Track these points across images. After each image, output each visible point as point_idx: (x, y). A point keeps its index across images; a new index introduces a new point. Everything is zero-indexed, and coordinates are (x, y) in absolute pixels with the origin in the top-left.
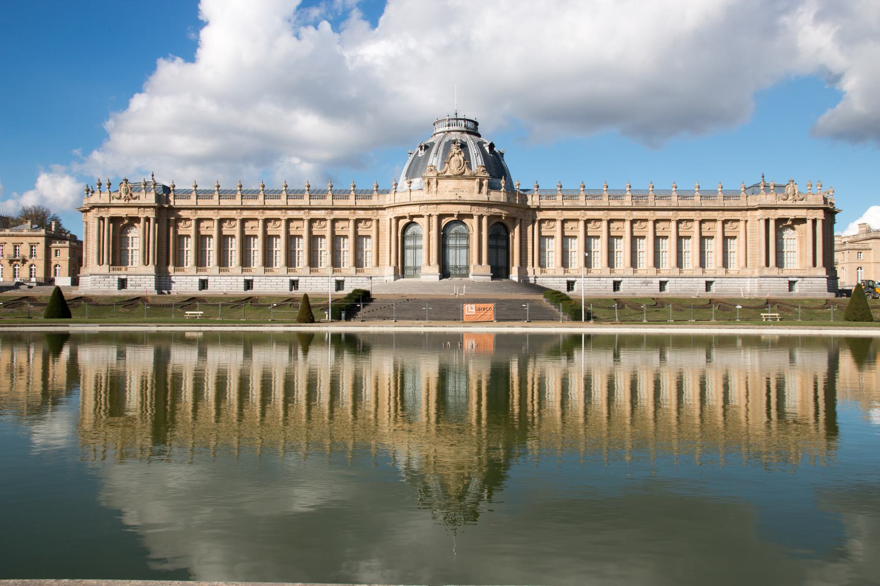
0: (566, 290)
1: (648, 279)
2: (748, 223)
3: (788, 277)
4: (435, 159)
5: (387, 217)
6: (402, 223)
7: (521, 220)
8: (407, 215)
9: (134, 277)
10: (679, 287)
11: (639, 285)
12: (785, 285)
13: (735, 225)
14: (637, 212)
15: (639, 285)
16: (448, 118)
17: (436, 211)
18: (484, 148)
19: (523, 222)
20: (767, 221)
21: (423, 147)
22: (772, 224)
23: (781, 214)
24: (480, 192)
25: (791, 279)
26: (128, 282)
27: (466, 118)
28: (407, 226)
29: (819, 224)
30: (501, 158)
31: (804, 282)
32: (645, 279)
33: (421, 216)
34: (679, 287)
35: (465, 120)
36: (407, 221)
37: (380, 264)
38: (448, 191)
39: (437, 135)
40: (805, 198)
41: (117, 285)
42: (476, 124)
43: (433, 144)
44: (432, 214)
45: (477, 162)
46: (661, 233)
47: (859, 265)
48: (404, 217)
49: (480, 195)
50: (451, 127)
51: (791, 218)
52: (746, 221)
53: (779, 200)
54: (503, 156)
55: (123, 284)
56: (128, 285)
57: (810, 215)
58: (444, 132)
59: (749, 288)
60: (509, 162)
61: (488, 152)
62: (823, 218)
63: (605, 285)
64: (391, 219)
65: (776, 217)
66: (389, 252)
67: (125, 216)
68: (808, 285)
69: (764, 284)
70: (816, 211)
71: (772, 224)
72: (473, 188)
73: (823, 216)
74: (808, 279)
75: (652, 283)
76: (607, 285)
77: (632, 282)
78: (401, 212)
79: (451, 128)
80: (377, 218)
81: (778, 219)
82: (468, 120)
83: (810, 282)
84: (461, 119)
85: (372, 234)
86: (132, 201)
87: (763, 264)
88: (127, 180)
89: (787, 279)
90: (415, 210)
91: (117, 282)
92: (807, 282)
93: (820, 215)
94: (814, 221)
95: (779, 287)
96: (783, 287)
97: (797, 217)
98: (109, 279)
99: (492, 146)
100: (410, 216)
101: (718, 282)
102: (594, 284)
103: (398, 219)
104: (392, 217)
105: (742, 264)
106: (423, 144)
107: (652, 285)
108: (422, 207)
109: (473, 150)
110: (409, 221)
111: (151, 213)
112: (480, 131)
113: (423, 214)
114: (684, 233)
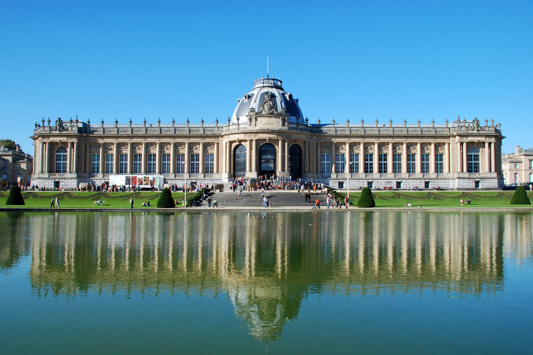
0: (338, 187)
1: (389, 180)
2: (451, 145)
3: (475, 179)
4: (255, 104)
5: (224, 141)
6: (234, 145)
7: (309, 143)
8: (237, 140)
9: (64, 180)
11: (384, 184)
15: (384, 184)
16: (263, 78)
17: (254, 137)
18: (286, 97)
19: (310, 144)
20: (462, 144)
21: (247, 97)
22: (464, 145)
23: (470, 139)
24: (283, 125)
25: (476, 180)
26: (60, 183)
27: (275, 78)
28: (237, 147)
29: (492, 146)
30: (296, 103)
31: (484, 181)
32: (387, 180)
33: (246, 141)
35: (273, 79)
36: (237, 143)
37: (219, 171)
38: (262, 124)
39: (256, 89)
41: (53, 185)
42: (281, 82)
43: (253, 94)
44: (253, 138)
45: (280, 106)
47: (516, 172)
48: (235, 141)
49: (283, 127)
50: (265, 84)
51: (476, 141)
52: (449, 144)
54: (298, 103)
55: (57, 184)
56: (60, 185)
57: (488, 140)
58: (261, 87)
59: (451, 185)
60: (301, 105)
61: (288, 100)
62: (495, 141)
63: (363, 184)
64: (226, 143)
65: (467, 141)
66: (225, 164)
67: (59, 141)
68: (487, 183)
69: (460, 183)
72: (279, 121)
76: (364, 184)
77: (380, 182)
78: (233, 138)
79: (265, 85)
80: (217, 142)
81: (468, 142)
82: (275, 80)
83: (488, 181)
84: (271, 79)
85: (214, 152)
86: (64, 132)
87: (459, 170)
88: (60, 119)
90: (242, 137)
91: (53, 183)
93: (493, 140)
94: (490, 144)
95: (470, 185)
96: (472, 185)
98: (48, 182)
99: (290, 96)
100: (238, 140)
101: (432, 182)
102: (355, 184)
103: (231, 143)
104: (227, 141)
106: (247, 95)
107: (392, 184)
108: (246, 135)
109: (278, 100)
110: (238, 143)
111: (75, 140)
112: (283, 87)
113: (246, 138)
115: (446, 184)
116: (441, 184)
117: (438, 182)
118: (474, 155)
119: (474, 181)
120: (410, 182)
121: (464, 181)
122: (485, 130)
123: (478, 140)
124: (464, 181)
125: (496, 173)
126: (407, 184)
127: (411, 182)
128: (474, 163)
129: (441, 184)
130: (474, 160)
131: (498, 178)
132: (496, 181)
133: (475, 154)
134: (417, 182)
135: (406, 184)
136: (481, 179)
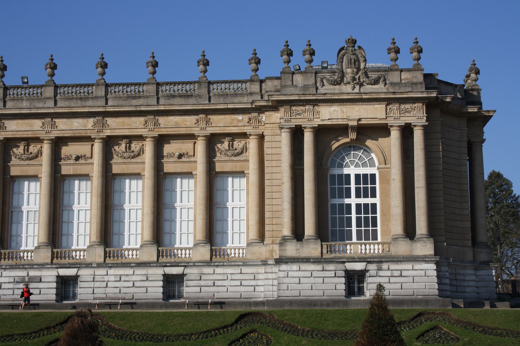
1: (33, 273)
10: (102, 290)
11: (11, 286)
12: (337, 280)
13: (241, 146)
14: (15, 122)
15: (11, 286)
22: (308, 138)
31: (381, 273)
34: (102, 290)
40: (382, 80)
46: (71, 167)
51: (351, 123)
53: (323, 85)
62: (424, 121)
65: (317, 122)
68: (392, 280)
69: (286, 280)
70: (408, 106)
71: (308, 138)
73: (425, 118)
74: (393, 266)
75: (40, 281)
83: (397, 273)
87: (287, 231)
89: (341, 266)
92: (389, 273)
97: (363, 122)
105: (253, 234)
107: (41, 285)
114: (125, 166)
115: (244, 283)
116: (225, 283)
117: (215, 277)
118: (357, 176)
119: (343, 274)
120: (106, 278)
121: (300, 274)
122: (385, 80)
123: (359, 120)
124: (300, 274)
125: (432, 239)
126: (97, 284)
127: (112, 278)
128: (358, 206)
129: (225, 283)
130: (358, 196)
131: (438, 258)
132: (429, 273)
133: (362, 171)
134: (134, 278)
135: (92, 284)
136: (369, 262)
